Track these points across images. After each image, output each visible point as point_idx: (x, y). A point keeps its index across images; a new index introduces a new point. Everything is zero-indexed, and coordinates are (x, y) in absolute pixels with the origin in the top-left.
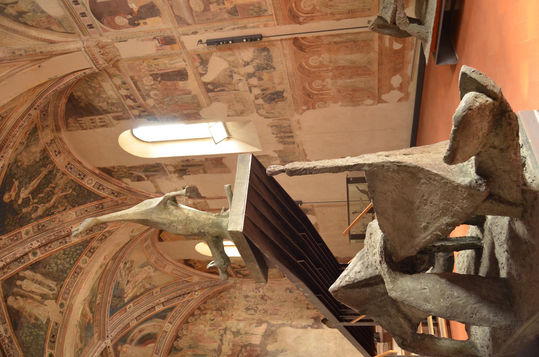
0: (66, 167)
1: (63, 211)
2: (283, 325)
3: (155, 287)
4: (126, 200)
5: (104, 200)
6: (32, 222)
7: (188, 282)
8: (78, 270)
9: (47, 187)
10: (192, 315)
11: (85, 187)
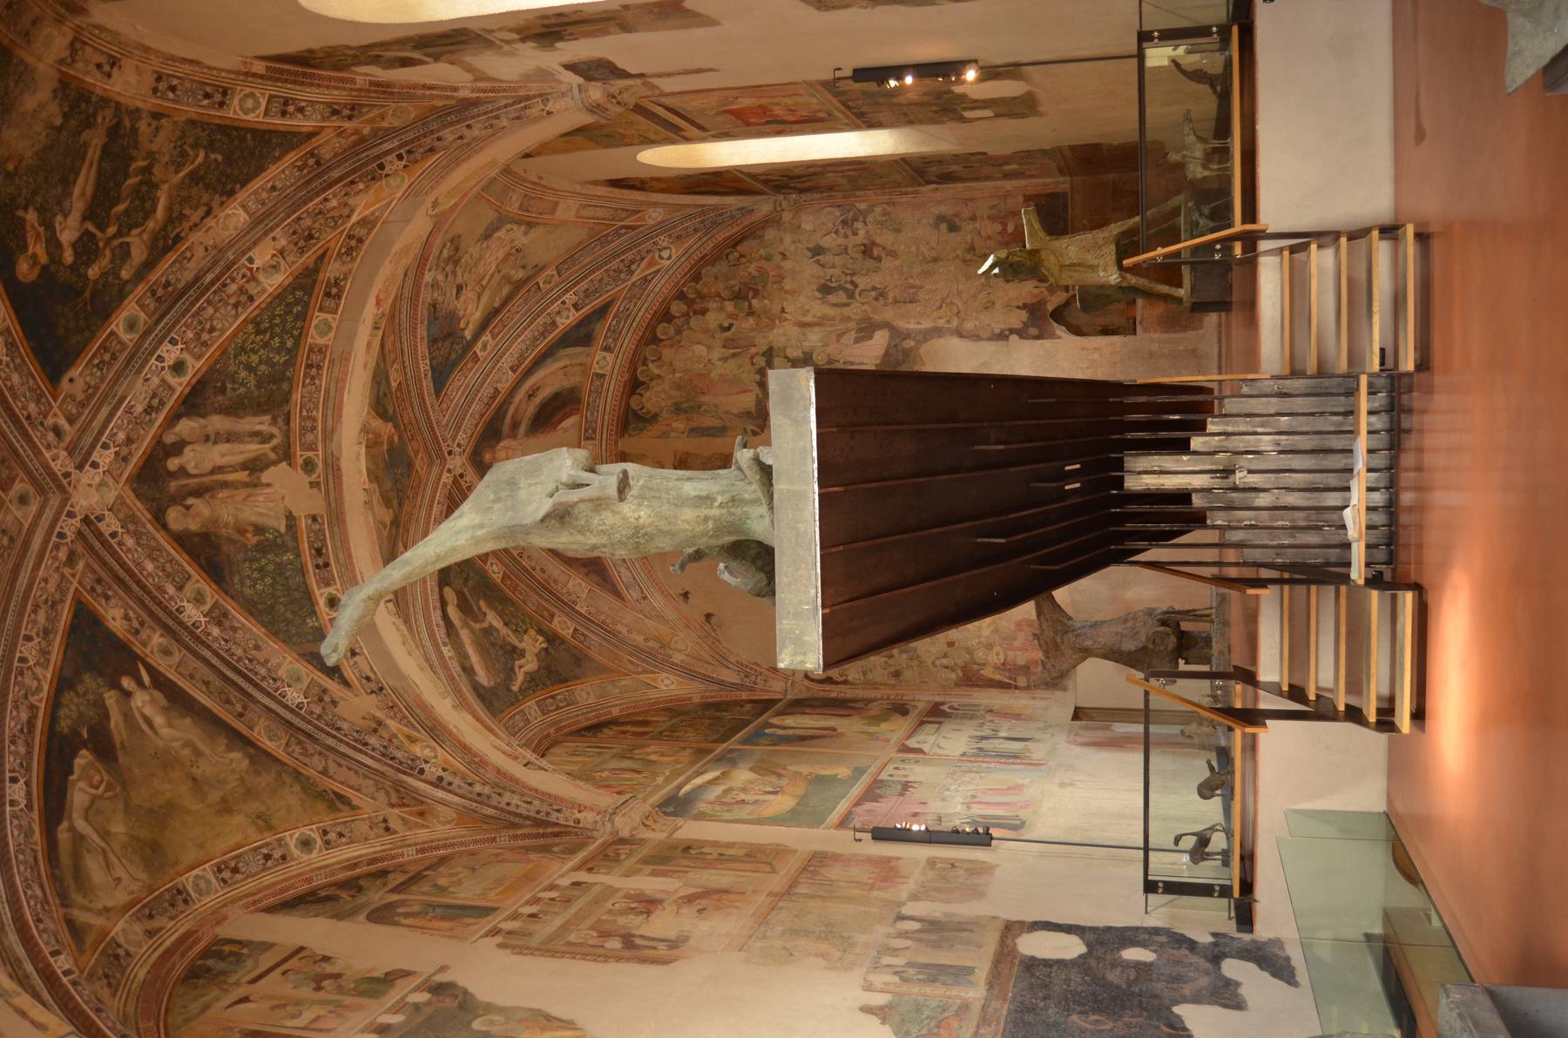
0: (155, 90)
1: (203, 218)
2: (937, 332)
3: (539, 269)
4: (383, 119)
5: (314, 140)
6: (132, 291)
7: (633, 228)
8: (315, 358)
9: (127, 176)
10: (665, 316)
11: (242, 125)
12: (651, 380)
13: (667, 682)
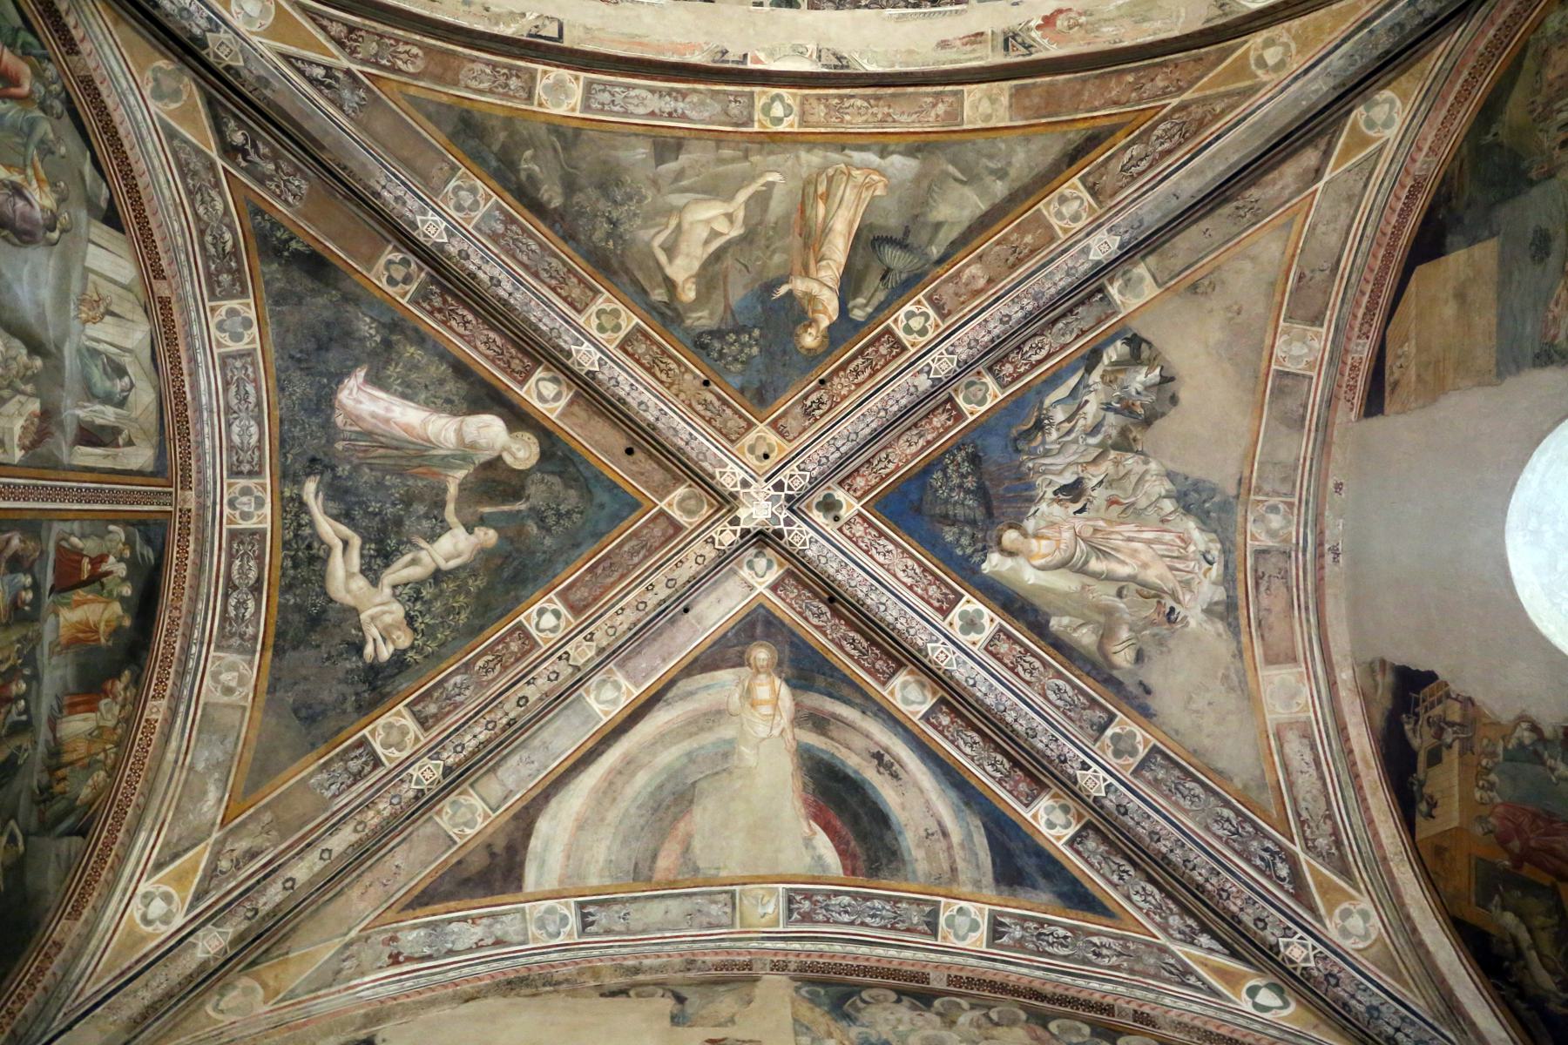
7: (1300, 891)
12: (939, 1014)
13: (157, 908)
